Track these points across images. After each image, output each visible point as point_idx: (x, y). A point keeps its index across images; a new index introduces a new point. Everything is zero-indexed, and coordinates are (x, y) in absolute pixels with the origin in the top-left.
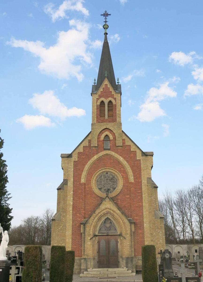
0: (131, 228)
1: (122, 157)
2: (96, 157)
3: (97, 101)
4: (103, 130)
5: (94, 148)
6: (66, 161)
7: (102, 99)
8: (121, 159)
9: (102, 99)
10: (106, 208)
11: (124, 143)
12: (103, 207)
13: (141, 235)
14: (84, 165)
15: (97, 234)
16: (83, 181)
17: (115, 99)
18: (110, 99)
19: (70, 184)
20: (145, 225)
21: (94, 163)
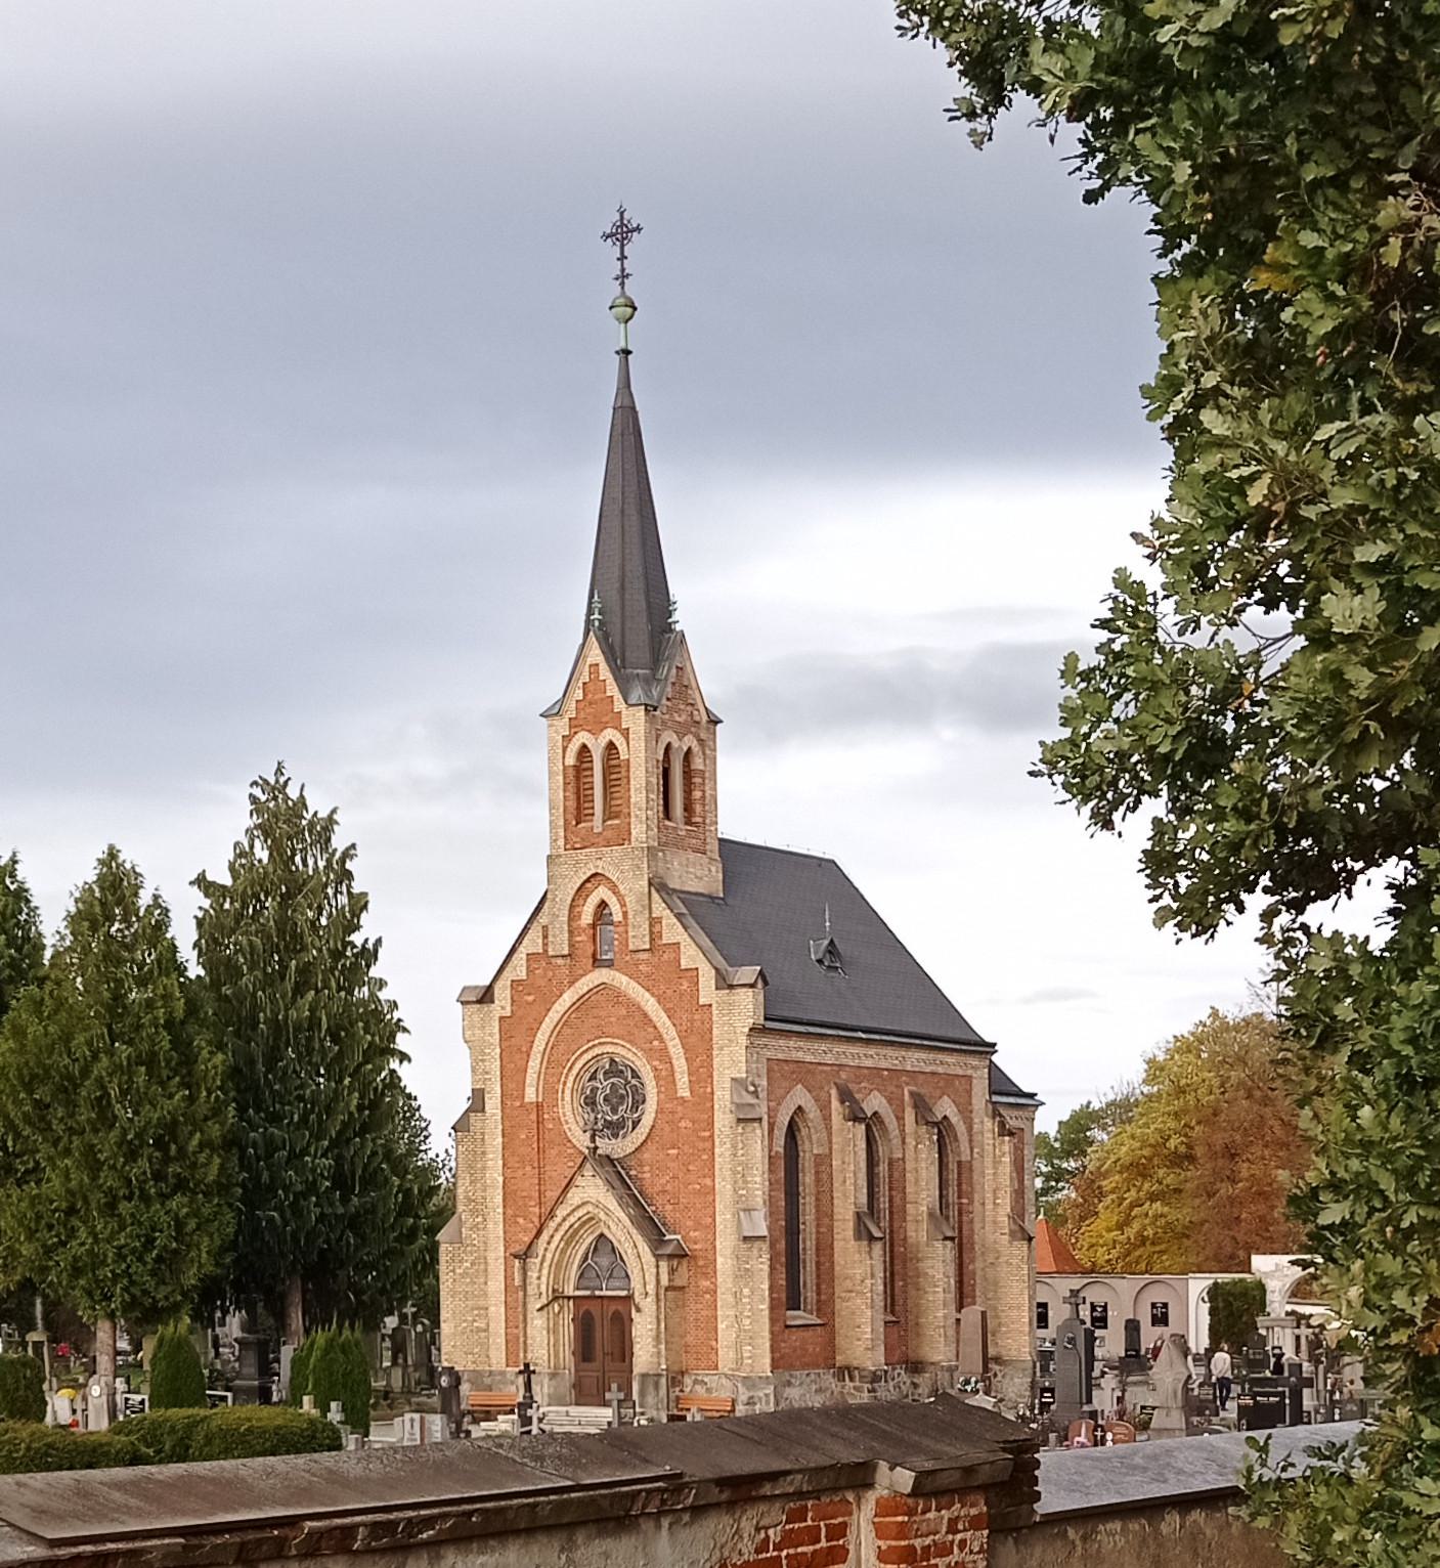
0: (658, 1273)
1: (653, 995)
2: (568, 998)
3: (565, 749)
4: (588, 880)
5: (560, 961)
6: (476, 1018)
7: (583, 737)
8: (650, 1004)
9: (583, 737)
10: (584, 1204)
11: (654, 936)
12: (574, 1197)
13: (708, 1296)
14: (533, 1032)
15: (570, 1291)
16: (531, 1095)
17: (626, 733)
18: (610, 734)
19: (493, 1104)
20: (720, 1260)
21: (564, 1022)
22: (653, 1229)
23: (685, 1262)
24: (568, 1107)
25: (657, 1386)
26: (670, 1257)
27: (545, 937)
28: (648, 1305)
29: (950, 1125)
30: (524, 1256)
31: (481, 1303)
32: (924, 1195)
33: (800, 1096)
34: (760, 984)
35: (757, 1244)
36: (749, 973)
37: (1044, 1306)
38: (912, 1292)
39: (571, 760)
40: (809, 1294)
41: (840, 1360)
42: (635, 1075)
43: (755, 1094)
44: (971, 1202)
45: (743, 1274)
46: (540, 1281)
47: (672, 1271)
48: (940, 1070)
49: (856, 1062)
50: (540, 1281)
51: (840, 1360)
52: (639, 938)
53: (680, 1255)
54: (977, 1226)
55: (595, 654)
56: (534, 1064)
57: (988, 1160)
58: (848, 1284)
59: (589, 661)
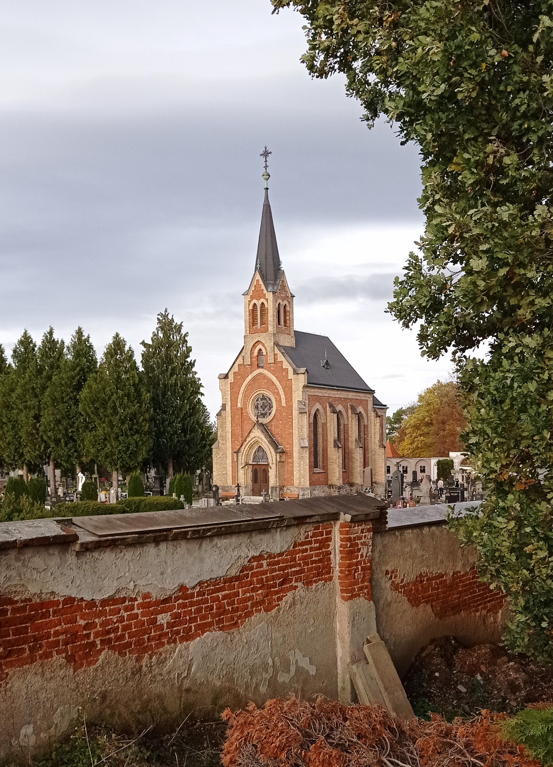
2: (250, 377)
5: (248, 366)
6: (223, 383)
7: (254, 301)
8: (274, 379)
9: (254, 301)
12: (252, 435)
14: (240, 387)
15: (251, 462)
16: (239, 405)
17: (267, 300)
18: (262, 300)
19: (228, 408)
20: (294, 454)
21: (249, 384)
22: (275, 445)
23: (284, 454)
24: (250, 409)
25: (276, 490)
26: (280, 453)
27: (243, 359)
28: (273, 467)
29: (362, 414)
30: (237, 452)
31: (225, 466)
32: (354, 434)
33: (318, 406)
34: (306, 373)
35: (305, 449)
36: (303, 370)
37: (389, 467)
38: (350, 463)
39: (251, 308)
40: (320, 463)
41: (329, 483)
42: (270, 400)
43: (305, 405)
44: (368, 437)
45: (301, 458)
46: (242, 459)
47: (280, 457)
48: (359, 398)
49: (334, 396)
50: (242, 459)
51: (329, 483)
52: (271, 360)
53: (283, 452)
54: (369, 444)
55: (258, 277)
56: (240, 396)
57: (373, 425)
58: (332, 461)
59: (256, 279)
